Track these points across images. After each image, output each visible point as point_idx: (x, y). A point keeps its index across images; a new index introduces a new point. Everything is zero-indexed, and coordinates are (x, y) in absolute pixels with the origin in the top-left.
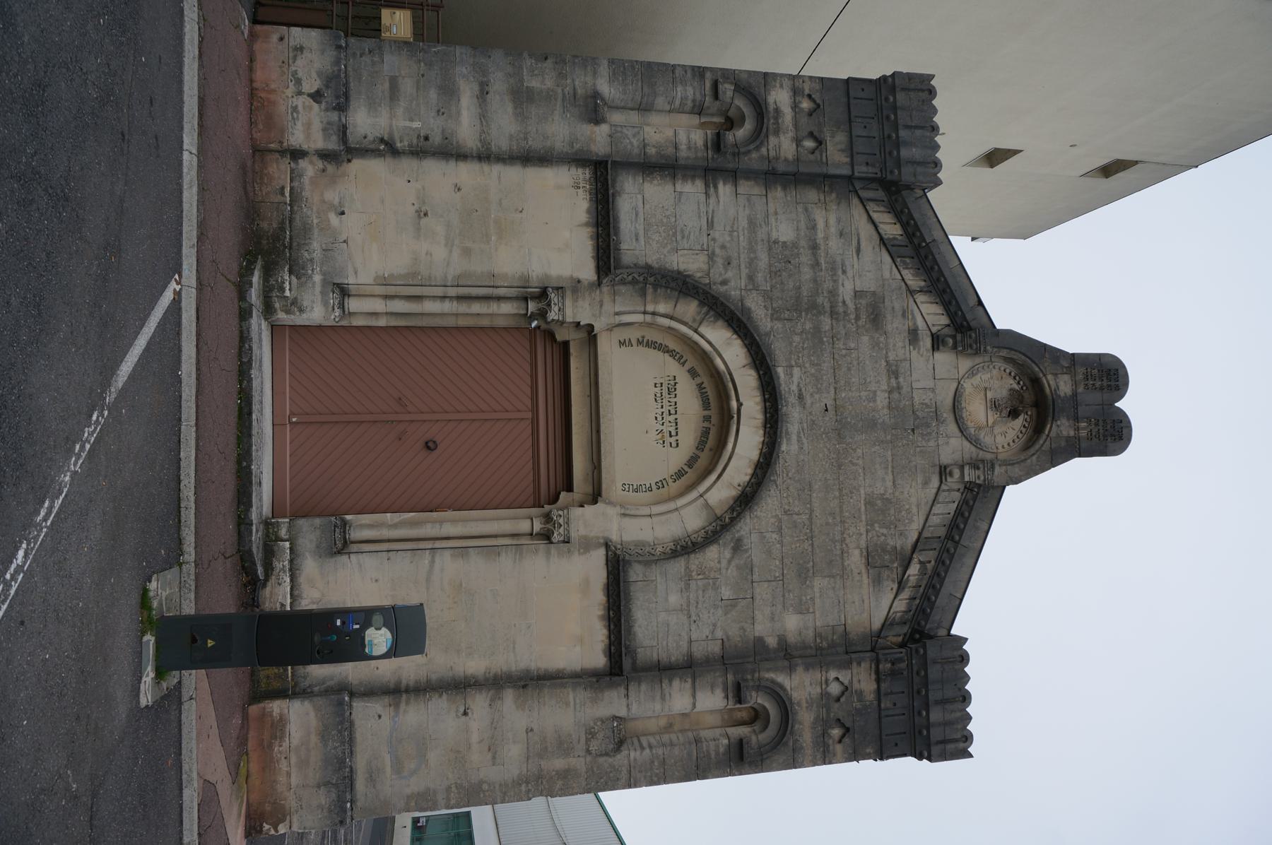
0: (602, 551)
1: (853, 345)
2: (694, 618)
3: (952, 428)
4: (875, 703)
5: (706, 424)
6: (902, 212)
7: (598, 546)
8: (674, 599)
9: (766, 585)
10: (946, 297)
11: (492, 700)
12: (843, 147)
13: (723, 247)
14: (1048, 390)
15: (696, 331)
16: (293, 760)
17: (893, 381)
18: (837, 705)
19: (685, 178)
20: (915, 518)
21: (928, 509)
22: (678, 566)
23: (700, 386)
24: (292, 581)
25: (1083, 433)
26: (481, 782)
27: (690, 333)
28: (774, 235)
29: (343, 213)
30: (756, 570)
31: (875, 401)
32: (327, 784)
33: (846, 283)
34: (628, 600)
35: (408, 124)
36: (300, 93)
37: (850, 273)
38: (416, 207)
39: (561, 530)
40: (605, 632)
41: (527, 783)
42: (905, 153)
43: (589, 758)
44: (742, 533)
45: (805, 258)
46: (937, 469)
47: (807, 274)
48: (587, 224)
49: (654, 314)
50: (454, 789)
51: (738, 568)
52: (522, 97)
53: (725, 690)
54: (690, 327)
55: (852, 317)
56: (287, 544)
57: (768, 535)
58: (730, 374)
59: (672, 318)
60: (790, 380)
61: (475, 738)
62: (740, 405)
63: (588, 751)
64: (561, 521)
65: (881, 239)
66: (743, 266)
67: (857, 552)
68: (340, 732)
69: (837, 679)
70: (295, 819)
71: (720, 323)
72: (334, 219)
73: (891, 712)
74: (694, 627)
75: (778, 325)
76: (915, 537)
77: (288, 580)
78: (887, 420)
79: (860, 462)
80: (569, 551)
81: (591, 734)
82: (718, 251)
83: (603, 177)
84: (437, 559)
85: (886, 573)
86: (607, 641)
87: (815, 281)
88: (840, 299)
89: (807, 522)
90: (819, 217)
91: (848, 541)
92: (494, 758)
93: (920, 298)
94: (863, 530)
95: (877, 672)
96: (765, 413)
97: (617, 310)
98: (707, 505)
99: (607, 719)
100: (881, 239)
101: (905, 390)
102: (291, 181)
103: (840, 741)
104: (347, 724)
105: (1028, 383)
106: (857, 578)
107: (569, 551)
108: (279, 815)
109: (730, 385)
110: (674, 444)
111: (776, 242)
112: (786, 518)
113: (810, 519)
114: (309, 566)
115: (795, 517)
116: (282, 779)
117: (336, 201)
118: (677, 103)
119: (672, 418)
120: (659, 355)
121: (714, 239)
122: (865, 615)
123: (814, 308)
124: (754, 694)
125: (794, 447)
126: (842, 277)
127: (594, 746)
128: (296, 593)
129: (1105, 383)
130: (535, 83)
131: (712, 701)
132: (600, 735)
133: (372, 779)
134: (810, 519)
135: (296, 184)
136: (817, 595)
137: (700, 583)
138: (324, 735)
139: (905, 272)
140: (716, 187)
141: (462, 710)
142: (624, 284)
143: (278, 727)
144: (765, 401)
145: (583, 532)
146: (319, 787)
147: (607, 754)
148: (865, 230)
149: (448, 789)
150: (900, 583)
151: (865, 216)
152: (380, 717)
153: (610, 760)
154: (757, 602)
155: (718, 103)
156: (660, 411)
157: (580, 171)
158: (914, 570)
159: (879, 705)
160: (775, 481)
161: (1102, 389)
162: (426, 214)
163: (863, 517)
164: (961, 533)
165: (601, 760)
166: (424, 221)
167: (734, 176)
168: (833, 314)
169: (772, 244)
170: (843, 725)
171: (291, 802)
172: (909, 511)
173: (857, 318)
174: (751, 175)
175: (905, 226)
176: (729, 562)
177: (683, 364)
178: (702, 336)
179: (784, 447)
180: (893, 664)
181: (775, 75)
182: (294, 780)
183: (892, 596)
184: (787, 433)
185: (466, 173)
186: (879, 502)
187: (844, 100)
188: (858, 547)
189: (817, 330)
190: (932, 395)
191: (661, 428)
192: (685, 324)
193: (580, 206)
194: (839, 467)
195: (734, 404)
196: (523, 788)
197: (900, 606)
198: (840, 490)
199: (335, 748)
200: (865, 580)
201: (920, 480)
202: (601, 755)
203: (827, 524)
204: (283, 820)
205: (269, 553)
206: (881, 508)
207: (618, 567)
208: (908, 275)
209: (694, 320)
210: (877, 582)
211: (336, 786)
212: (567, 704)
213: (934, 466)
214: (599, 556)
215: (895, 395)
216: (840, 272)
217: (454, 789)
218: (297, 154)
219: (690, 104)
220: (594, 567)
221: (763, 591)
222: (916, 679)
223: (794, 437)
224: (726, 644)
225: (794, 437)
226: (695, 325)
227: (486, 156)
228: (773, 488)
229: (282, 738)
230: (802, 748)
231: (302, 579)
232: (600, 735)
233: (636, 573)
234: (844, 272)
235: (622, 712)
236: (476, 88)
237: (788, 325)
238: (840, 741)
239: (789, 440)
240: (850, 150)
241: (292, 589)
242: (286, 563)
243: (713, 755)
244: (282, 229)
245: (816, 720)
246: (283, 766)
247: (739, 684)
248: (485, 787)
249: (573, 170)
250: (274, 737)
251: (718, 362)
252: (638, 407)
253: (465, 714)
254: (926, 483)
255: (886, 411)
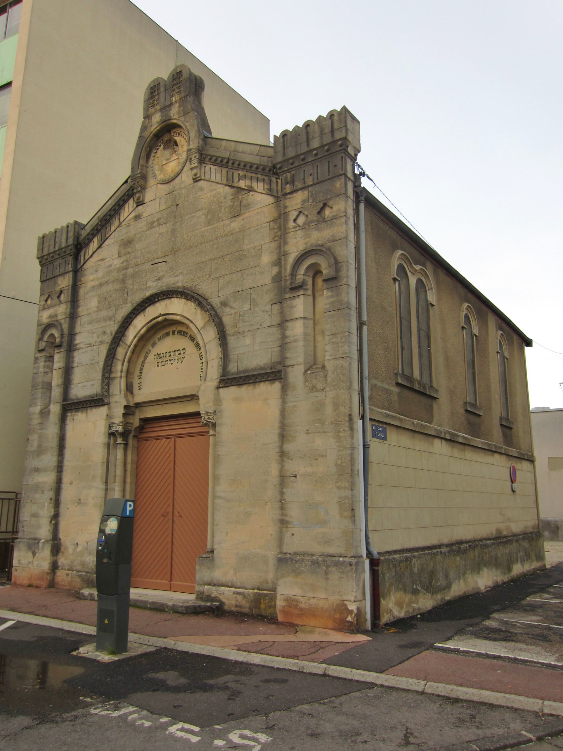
0: (221, 390)
1: (140, 253)
2: (258, 326)
3: (177, 180)
4: (310, 189)
5: (176, 333)
6: (88, 239)
7: (218, 394)
8: (248, 341)
9: (245, 281)
10: (121, 203)
11: (289, 458)
12: (63, 278)
13: (98, 337)
14: (158, 128)
15: (129, 347)
16: (310, 595)
17: (156, 224)
18: (309, 216)
19: (73, 362)
20: (218, 191)
21: (213, 184)
22: (232, 341)
23: (160, 339)
24: (224, 586)
25: (178, 97)
26: (337, 465)
27: (130, 349)
28: (95, 309)
29: (77, 544)
30: (237, 290)
31: (163, 233)
32: (326, 573)
33: (115, 264)
34: (246, 371)
35: (46, 508)
36: (33, 562)
37: (111, 262)
38: (76, 504)
39: (211, 417)
40: (262, 384)
41: (339, 432)
42: (63, 245)
43: (328, 389)
44: (218, 303)
45: (105, 289)
46: (196, 184)
47: (110, 287)
48: (87, 413)
49: (122, 372)
50: (339, 484)
51: (235, 301)
52: (40, 451)
53: (294, 298)
54: (128, 350)
55: (128, 256)
56: (206, 587)
57: (220, 285)
58: (148, 323)
59: (124, 361)
60: (153, 288)
61: (309, 470)
62: (161, 315)
63: (323, 390)
64: (206, 418)
65: (99, 248)
66: (106, 324)
67: (232, 225)
68: (296, 562)
69: (295, 220)
70: (346, 598)
71: (126, 333)
72: (79, 549)
73: (315, 176)
74: (264, 325)
75: (129, 299)
76: (227, 188)
77: (223, 588)
78: (171, 223)
79: (190, 234)
80: (220, 412)
81: (313, 389)
82: (99, 340)
83: (70, 406)
84: (219, 494)
85: (244, 202)
86: (267, 383)
87: (113, 282)
88: (121, 265)
89: (216, 261)
90: (90, 285)
91: (226, 232)
92: (322, 456)
93: (122, 219)
94: (222, 223)
95: (291, 193)
96: (164, 299)
97: (118, 393)
98: (204, 327)
99: (305, 378)
100: (99, 248)
101: (159, 216)
102: (65, 570)
103: (332, 208)
104: (293, 557)
105: (159, 140)
106: (245, 220)
107: (220, 412)
108: (342, 608)
109: (152, 323)
110: (184, 351)
111: (98, 308)
112: (212, 276)
113: (214, 259)
114: (218, 575)
115: (213, 269)
116: (321, 603)
117: (73, 547)
118: (47, 370)
119: (172, 354)
120: (146, 365)
121: (96, 342)
122: (266, 209)
123: (123, 281)
124: (298, 277)
125: (180, 278)
126: (113, 267)
127: (320, 386)
128: (230, 584)
129: (156, 93)
130: (36, 444)
131: (299, 306)
132: (314, 382)
133: (328, 542)
134: (214, 259)
135: (66, 568)
136: (252, 245)
137: (241, 325)
138: (297, 573)
139: (112, 231)
140: (77, 345)
141: (293, 478)
142: (109, 390)
143: (291, 602)
144: (159, 300)
145: (211, 404)
146: (327, 579)
147: (326, 376)
148: (96, 257)
149: (339, 488)
150: (250, 191)
151: (91, 259)
152: (293, 534)
153: (330, 373)
154: (254, 285)
155: (46, 349)
156: (169, 362)
157: (68, 418)
158: (242, 184)
159: (311, 186)
160: (195, 286)
161: (159, 94)
162: (80, 500)
163: (216, 225)
164: (223, 159)
165: (329, 379)
166: (82, 501)
167: (72, 335)
168: (126, 268)
169: (99, 310)
170: (323, 209)
171: (334, 599)
172: (214, 196)
173: (129, 253)
174: (72, 326)
175: (94, 236)
176: (231, 308)
177: (150, 351)
178: (132, 342)
179: (180, 284)
180: (288, 183)
181: (38, 321)
182: (323, 595)
183: (257, 194)
184: (174, 284)
185: (66, 478)
186: (209, 217)
187: (47, 281)
188: (230, 225)
189: (133, 276)
190: (163, 198)
191: (176, 360)
192: (126, 353)
193: (80, 416)
194: (191, 247)
195: (160, 319)
196: (341, 434)
197: (260, 187)
198: (202, 243)
199: (306, 565)
200: (247, 214)
201: (200, 194)
202: (326, 380)
203: (217, 248)
204: (346, 605)
205: (209, 598)
206: (212, 216)
207: (228, 380)
208: (113, 228)
209: (125, 348)
210: (248, 206)
211: (328, 566)
212: (294, 406)
213: (194, 187)
214: (223, 392)
215: (161, 221)
216: (111, 268)
217: (339, 484)
218: (54, 566)
219: (47, 363)
220: (230, 393)
221: (248, 284)
222: (296, 164)
223: (176, 279)
224: (274, 302)
225: (176, 279)
226: (127, 347)
227: (60, 468)
228: (198, 287)
229: (297, 601)
230: (333, 236)
231: (223, 580)
232: (314, 382)
233: (233, 368)
234: (111, 266)
235: (302, 368)
236: (36, 474)
237: (130, 293)
238: (332, 208)
239: (177, 282)
240: (63, 274)
241: (228, 587)
242: (214, 588)
243: (332, 299)
244: (80, 576)
245: (318, 229)
246: (313, 602)
247: (291, 289)
248: (339, 462)
249: (68, 422)
250: (296, 606)
251: (142, 332)
252: (166, 376)
253: (295, 476)
254: (201, 189)
255: (168, 225)
